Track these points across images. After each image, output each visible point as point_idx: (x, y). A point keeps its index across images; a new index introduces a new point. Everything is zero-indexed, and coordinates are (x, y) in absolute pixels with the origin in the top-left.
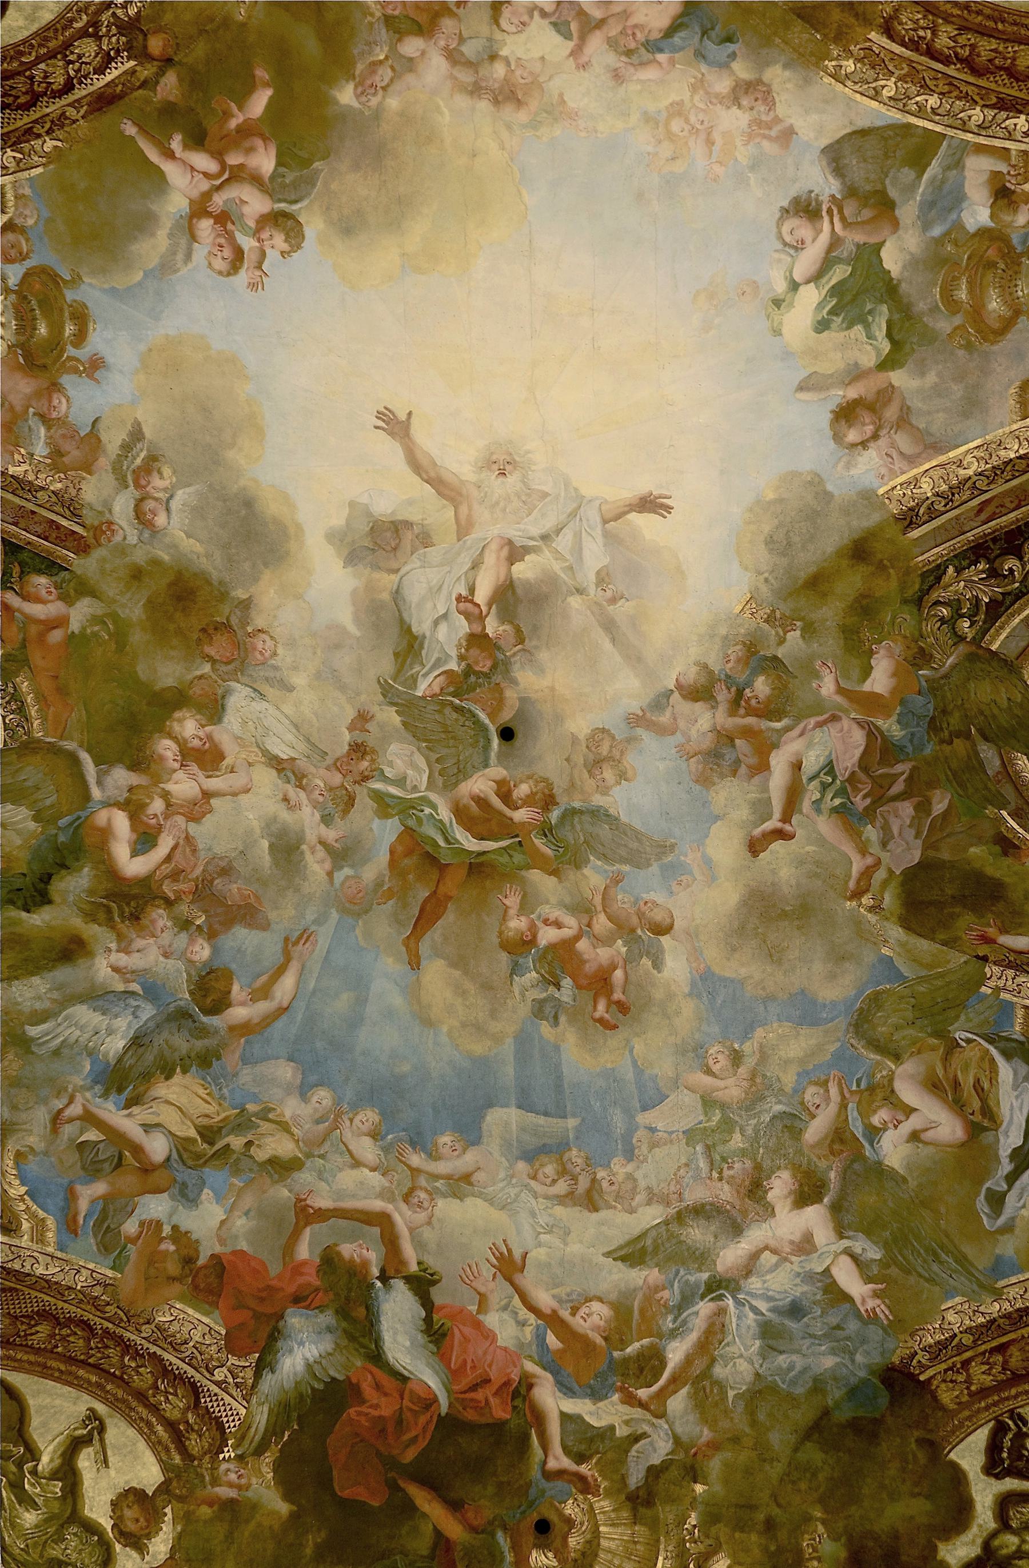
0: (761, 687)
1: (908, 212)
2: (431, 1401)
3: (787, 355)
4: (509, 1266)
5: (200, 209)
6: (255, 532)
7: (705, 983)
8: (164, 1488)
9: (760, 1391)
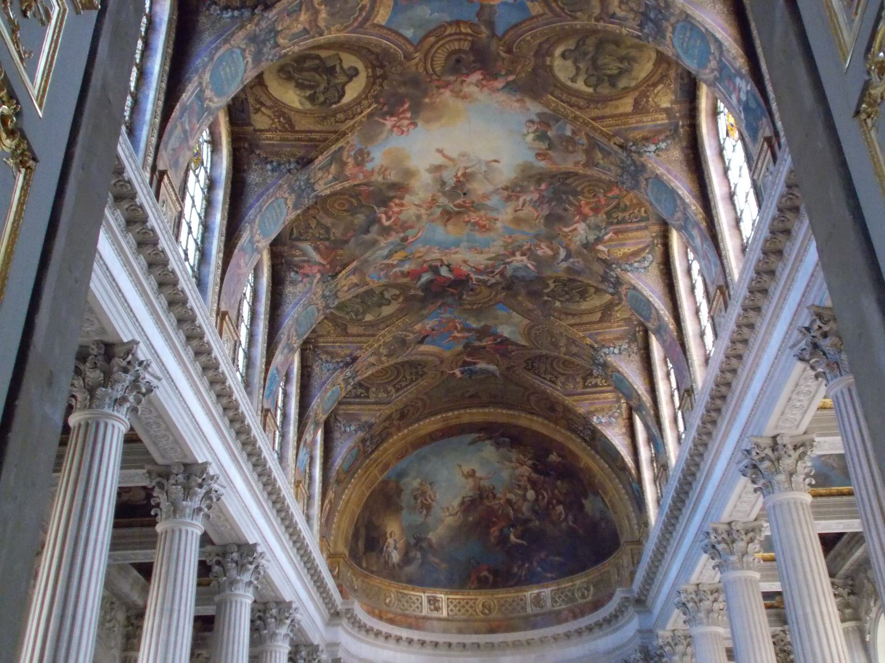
0: (518, 189)
1: (554, 128)
2: (449, 279)
3: (526, 143)
4: (465, 262)
5: (394, 126)
6: (409, 174)
7: (505, 227)
8: (401, 294)
9: (512, 276)
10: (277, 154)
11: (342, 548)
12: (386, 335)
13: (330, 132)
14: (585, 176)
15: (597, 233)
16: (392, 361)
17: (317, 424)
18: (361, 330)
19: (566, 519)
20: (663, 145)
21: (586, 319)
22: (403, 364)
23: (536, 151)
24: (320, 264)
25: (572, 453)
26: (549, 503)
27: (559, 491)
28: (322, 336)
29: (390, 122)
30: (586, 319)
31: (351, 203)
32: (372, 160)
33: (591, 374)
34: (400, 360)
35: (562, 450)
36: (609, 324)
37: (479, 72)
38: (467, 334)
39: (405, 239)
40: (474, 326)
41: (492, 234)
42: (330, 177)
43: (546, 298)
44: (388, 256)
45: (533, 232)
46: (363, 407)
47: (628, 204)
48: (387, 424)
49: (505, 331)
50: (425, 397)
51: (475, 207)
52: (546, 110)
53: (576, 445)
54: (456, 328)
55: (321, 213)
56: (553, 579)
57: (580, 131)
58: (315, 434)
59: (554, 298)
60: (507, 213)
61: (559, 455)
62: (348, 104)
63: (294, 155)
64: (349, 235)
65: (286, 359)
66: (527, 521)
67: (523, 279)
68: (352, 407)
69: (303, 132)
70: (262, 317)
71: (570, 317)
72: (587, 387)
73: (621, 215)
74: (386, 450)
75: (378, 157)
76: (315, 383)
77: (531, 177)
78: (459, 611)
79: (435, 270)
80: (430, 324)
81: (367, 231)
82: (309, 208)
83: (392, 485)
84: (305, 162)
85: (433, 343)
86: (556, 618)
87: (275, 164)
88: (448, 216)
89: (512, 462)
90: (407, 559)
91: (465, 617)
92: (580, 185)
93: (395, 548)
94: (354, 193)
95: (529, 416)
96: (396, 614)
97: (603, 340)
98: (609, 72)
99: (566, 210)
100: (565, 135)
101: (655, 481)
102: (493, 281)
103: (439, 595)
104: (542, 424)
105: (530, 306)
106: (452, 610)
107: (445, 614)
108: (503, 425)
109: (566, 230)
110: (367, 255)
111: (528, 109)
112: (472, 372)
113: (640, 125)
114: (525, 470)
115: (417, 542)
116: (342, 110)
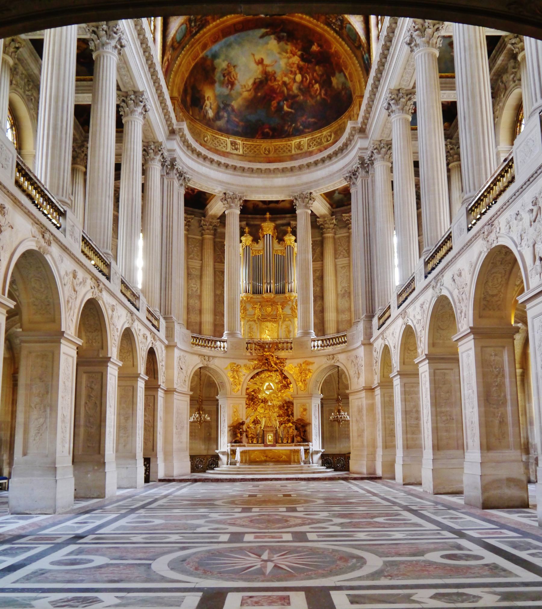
19: (320, 94)
26: (310, 83)
27: (317, 74)
56: (309, 132)
78: (250, 151)
89: (287, 53)
90: (218, 117)
91: (253, 155)
103: (238, 141)
106: (246, 151)
107: (241, 152)
115: (224, 105)
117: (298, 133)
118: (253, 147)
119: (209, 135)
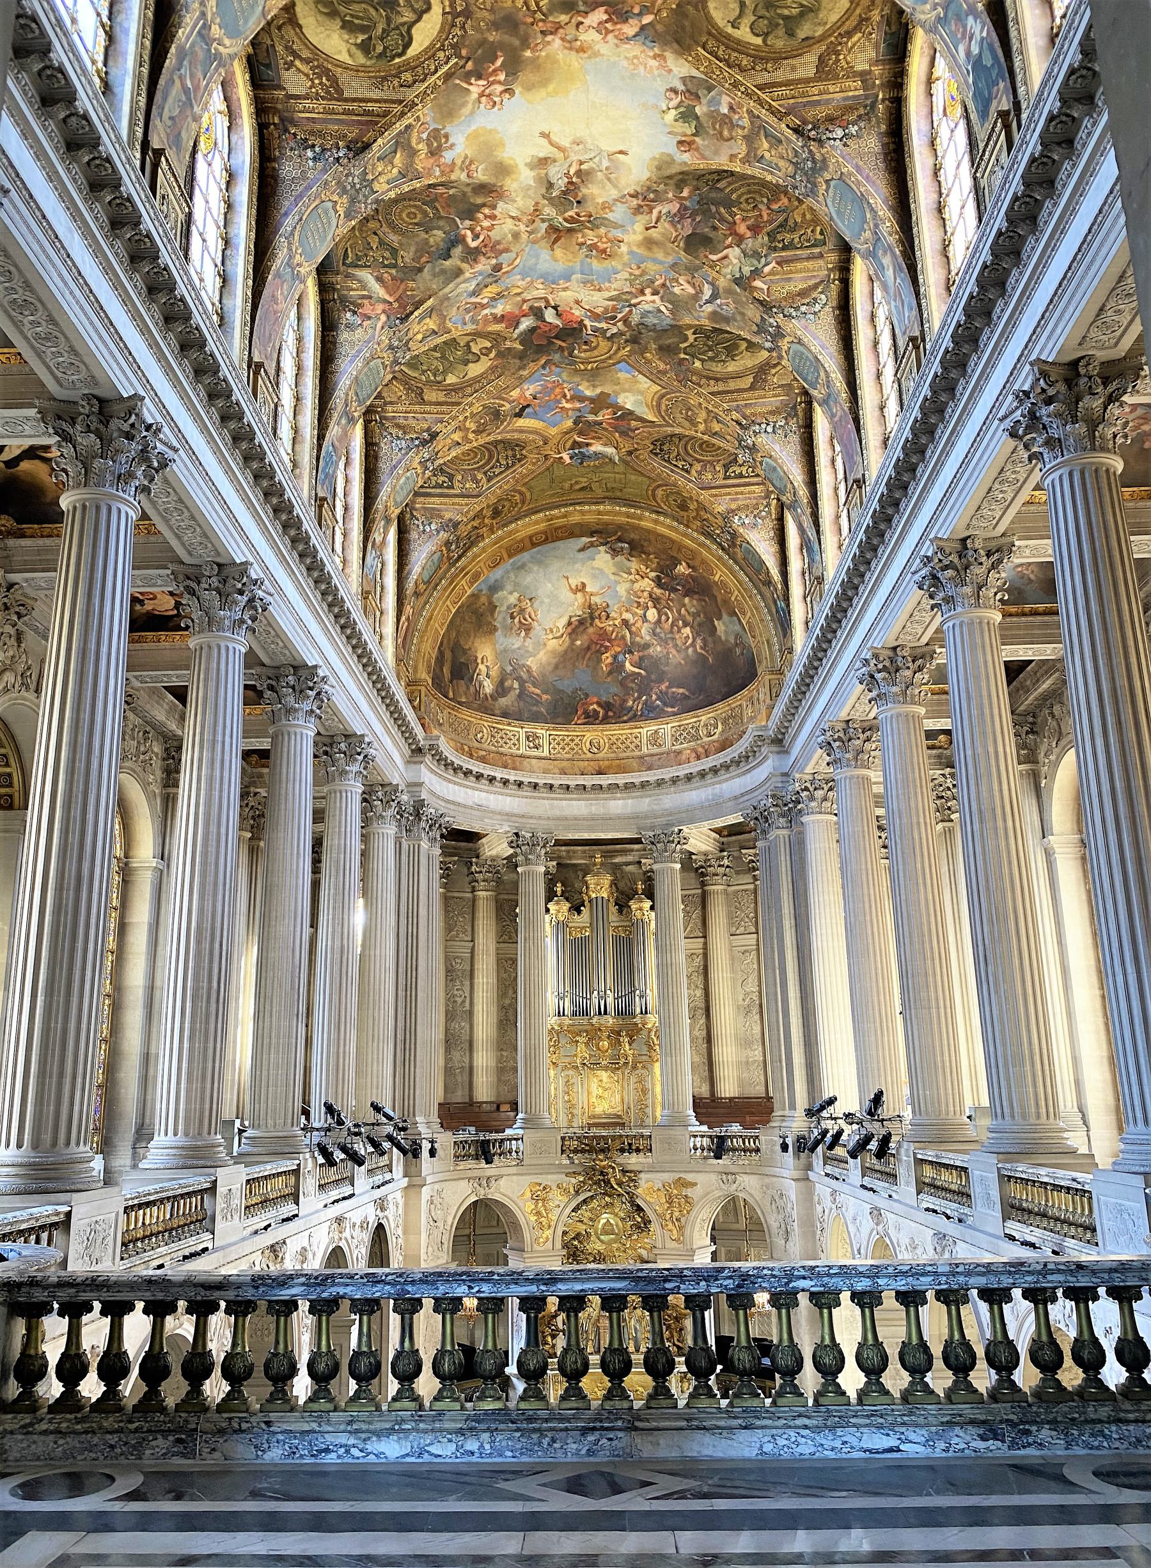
0: (652, 196)
1: (704, 101)
4: (577, 302)
5: (481, 95)
6: (503, 169)
7: (631, 253)
10: (321, 134)
11: (424, 676)
12: (476, 405)
13: (393, 102)
14: (744, 177)
15: (755, 262)
16: (483, 439)
17: (388, 520)
18: (441, 397)
19: (693, 645)
20: (853, 129)
21: (732, 385)
22: (495, 443)
23: (679, 138)
24: (385, 301)
25: (703, 562)
28: (391, 403)
29: (476, 87)
30: (732, 385)
31: (425, 214)
32: (453, 145)
33: (736, 461)
34: (491, 438)
35: (692, 559)
36: (762, 393)
37: (602, 9)
38: (578, 405)
39: (497, 268)
40: (588, 393)
41: (614, 263)
42: (395, 171)
43: (682, 356)
44: (474, 293)
45: (670, 260)
46: (446, 500)
47: (799, 220)
48: (476, 523)
49: (628, 401)
50: (524, 489)
51: (594, 223)
52: (695, 73)
53: (710, 553)
54: (565, 396)
55: (385, 228)
56: (674, 714)
57: (740, 106)
58: (386, 533)
59: (693, 356)
60: (635, 232)
61: (689, 566)
62: (417, 57)
63: (345, 136)
64: (424, 259)
65: (345, 433)
66: (647, 646)
67: (653, 328)
68: (432, 500)
69: (354, 100)
70: (310, 373)
71: (712, 382)
72: (729, 477)
73: (788, 237)
74: (476, 556)
75: (460, 143)
76: (384, 466)
77: (670, 177)
79: (538, 313)
80: (530, 389)
81: (447, 256)
82: (366, 219)
83: (483, 599)
84: (359, 148)
85: (535, 415)
86: (676, 757)
87: (317, 149)
88: (556, 234)
90: (501, 690)
92: (736, 190)
93: (488, 676)
94: (428, 197)
95: (654, 516)
96: (490, 752)
97: (754, 415)
98: (786, 12)
99: (715, 228)
100: (717, 111)
101: (805, 598)
102: (615, 330)
104: (670, 527)
105: (662, 366)
107: (546, 753)
108: (620, 527)
109: (714, 257)
110: (447, 290)
111: (670, 71)
112: (583, 457)
113: (825, 97)
114: (647, 584)
116: (408, 67)
117: (651, 713)
118: (567, 740)
119: (484, 725)
